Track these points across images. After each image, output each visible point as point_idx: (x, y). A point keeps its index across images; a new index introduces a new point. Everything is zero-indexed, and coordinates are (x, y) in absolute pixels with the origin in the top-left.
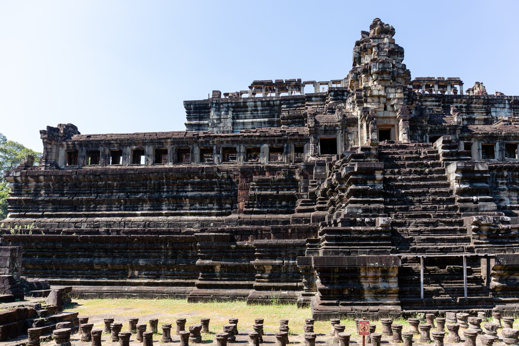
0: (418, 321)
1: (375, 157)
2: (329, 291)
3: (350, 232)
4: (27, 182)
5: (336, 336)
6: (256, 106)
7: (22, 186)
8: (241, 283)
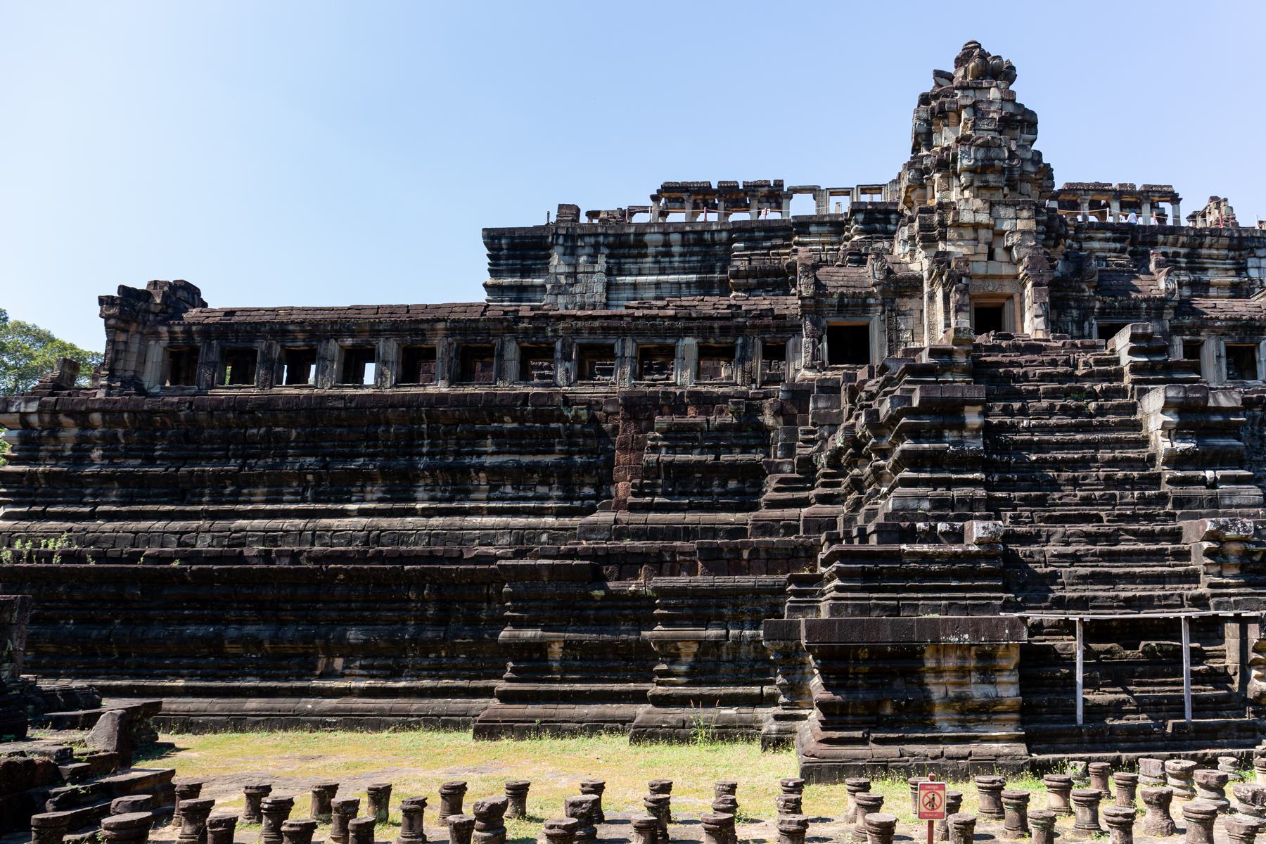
0: (1069, 783)
1: (965, 371)
2: (843, 706)
3: (898, 556)
4: (55, 427)
5: (860, 822)
7: (40, 437)
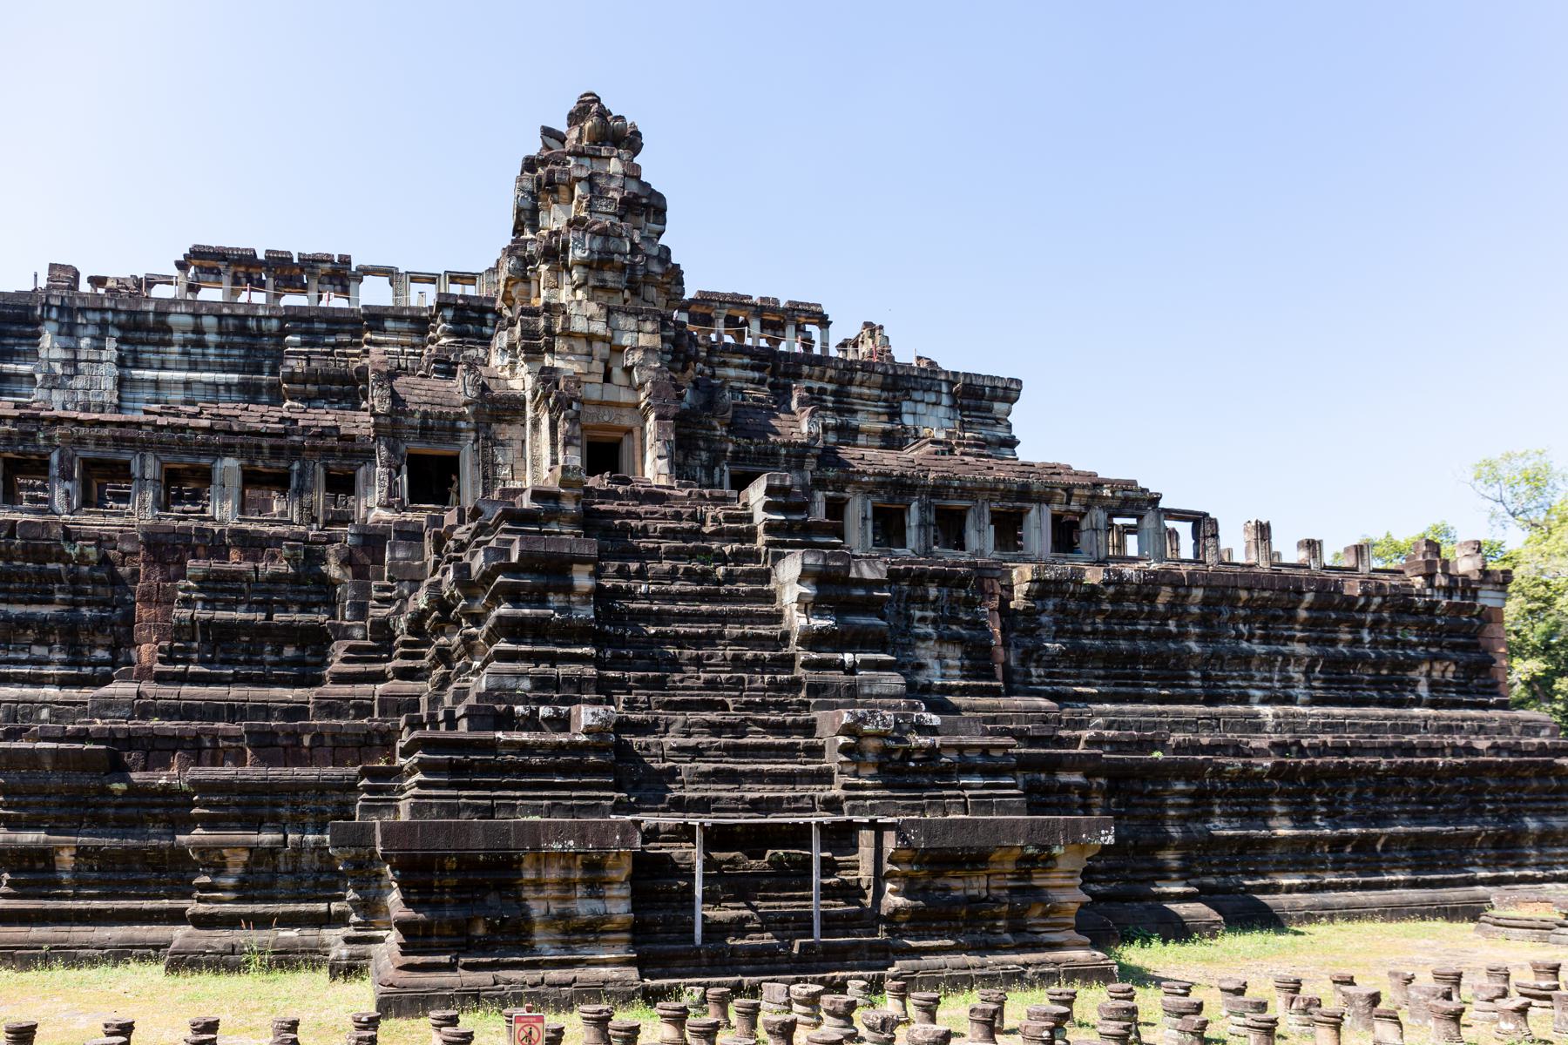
2: (427, 926)
3: (492, 746)
8: (147, 904)
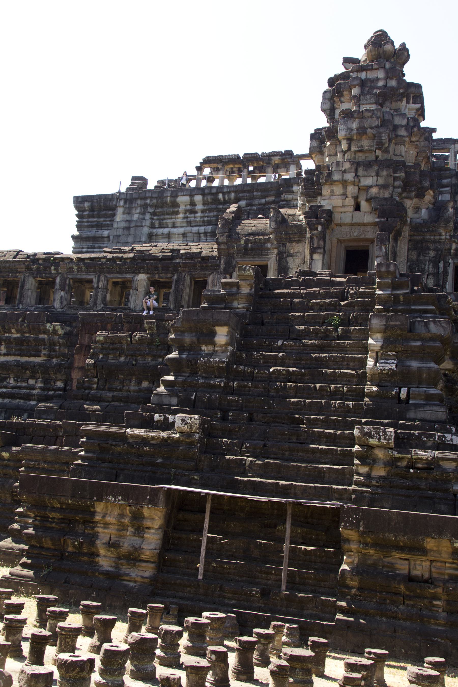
6: (193, 204)
